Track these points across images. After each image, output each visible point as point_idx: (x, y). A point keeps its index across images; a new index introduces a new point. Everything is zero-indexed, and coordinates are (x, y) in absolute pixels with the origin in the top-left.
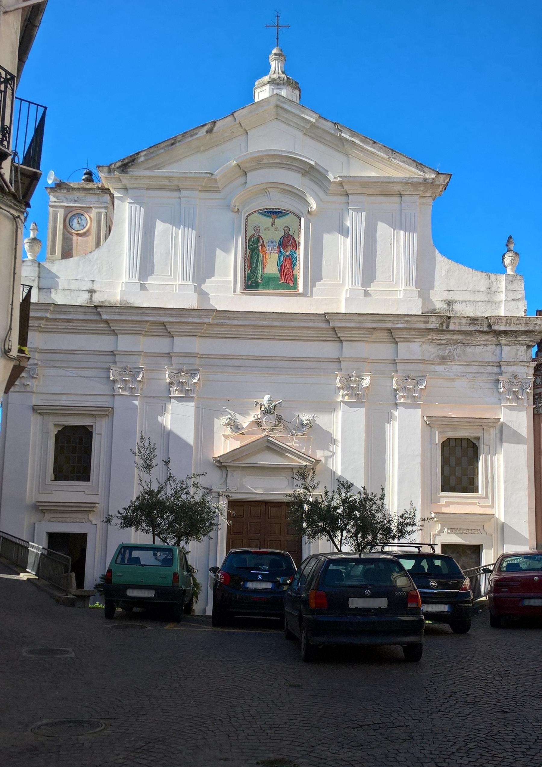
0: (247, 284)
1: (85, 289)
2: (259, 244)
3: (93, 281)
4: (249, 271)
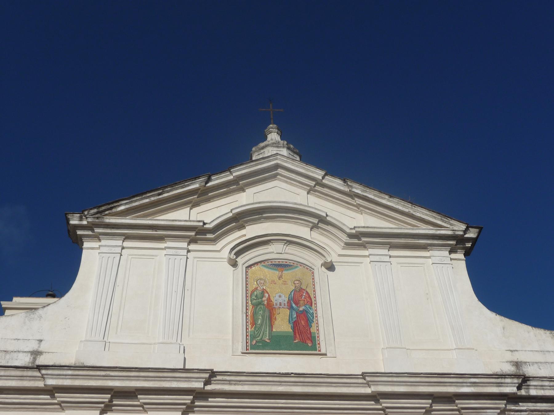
0: (251, 345)
1: (27, 349)
2: (264, 299)
3: (41, 341)
4: (253, 329)
